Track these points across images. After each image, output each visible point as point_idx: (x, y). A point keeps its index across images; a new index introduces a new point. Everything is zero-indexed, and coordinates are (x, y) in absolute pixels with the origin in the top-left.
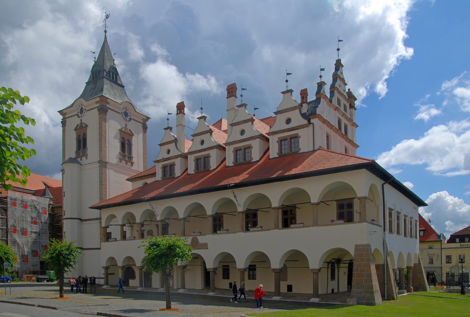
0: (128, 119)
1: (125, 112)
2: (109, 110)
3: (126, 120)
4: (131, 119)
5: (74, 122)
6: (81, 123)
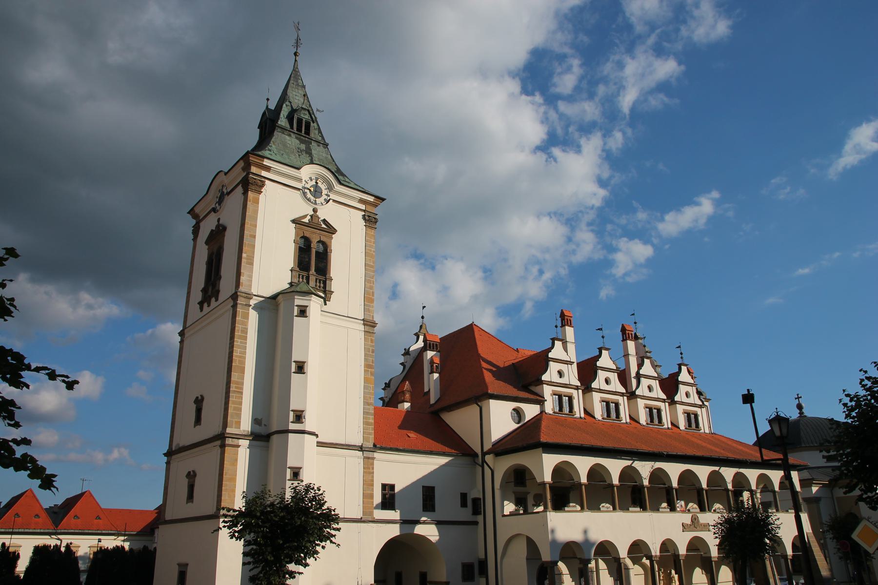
6: (218, 226)
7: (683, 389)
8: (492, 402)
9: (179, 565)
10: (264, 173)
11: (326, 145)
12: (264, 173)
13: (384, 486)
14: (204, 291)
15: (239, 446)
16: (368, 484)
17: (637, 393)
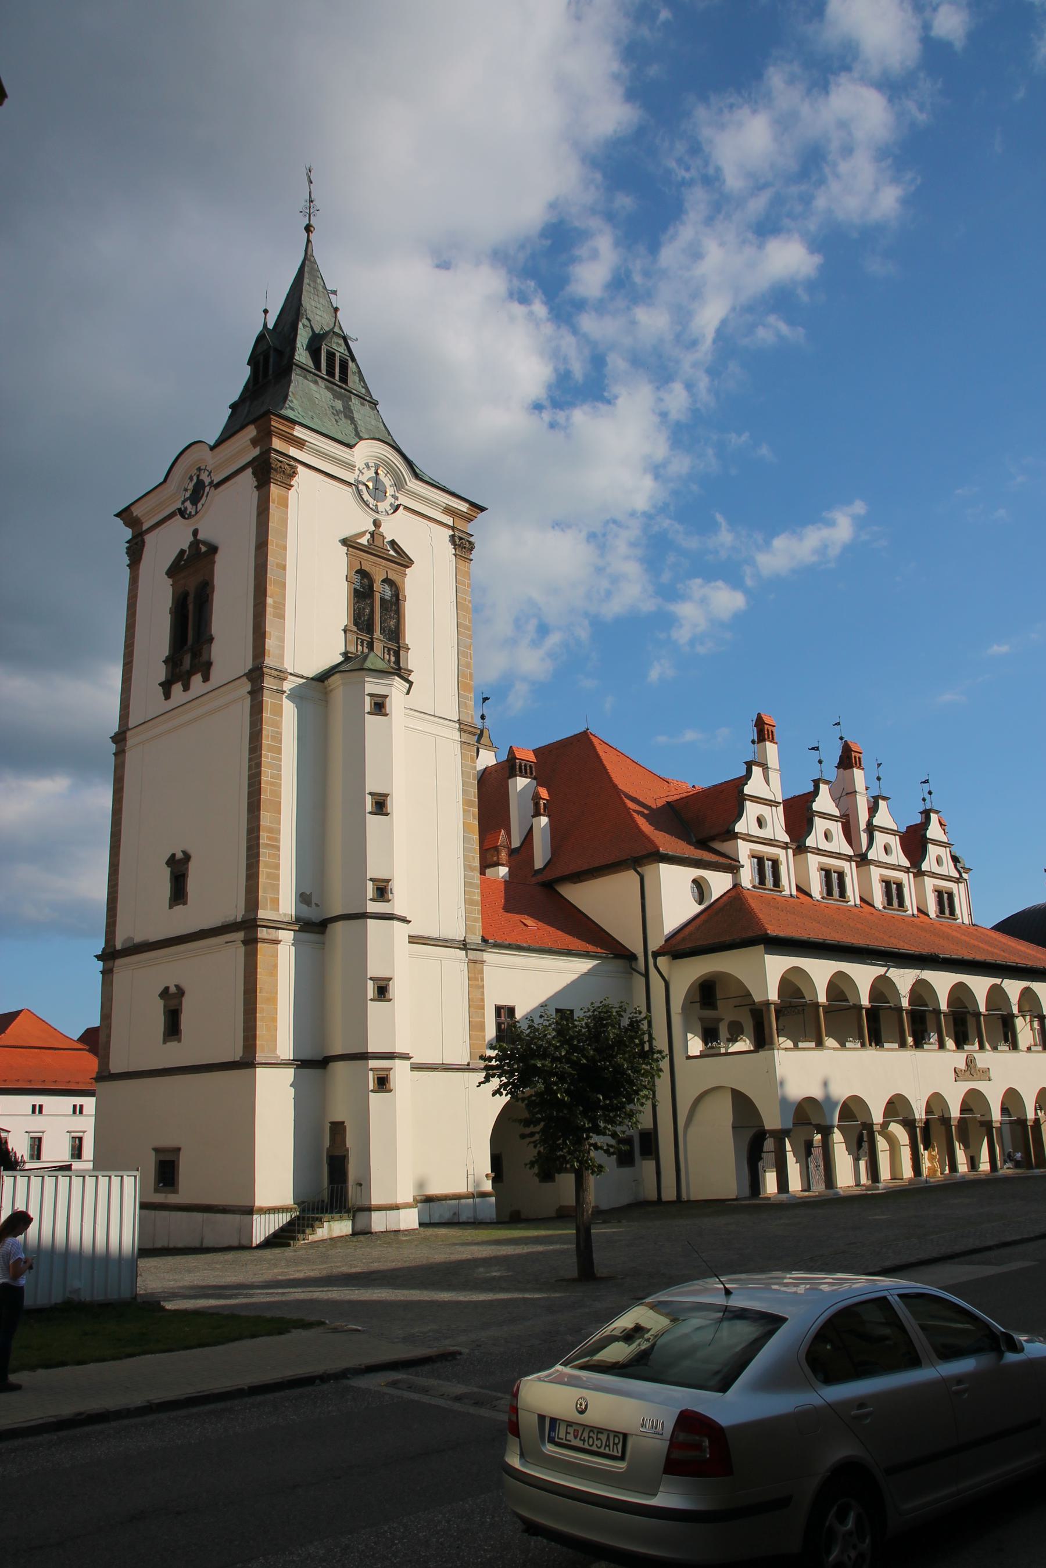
2: (300, 469)
6: (196, 543)
7: (933, 850)
8: (663, 867)
9: (157, 1150)
10: (293, 452)
11: (374, 404)
12: (293, 452)
13: (499, 1009)
14: (172, 661)
15: (278, 942)
16: (476, 1005)
17: (871, 855)
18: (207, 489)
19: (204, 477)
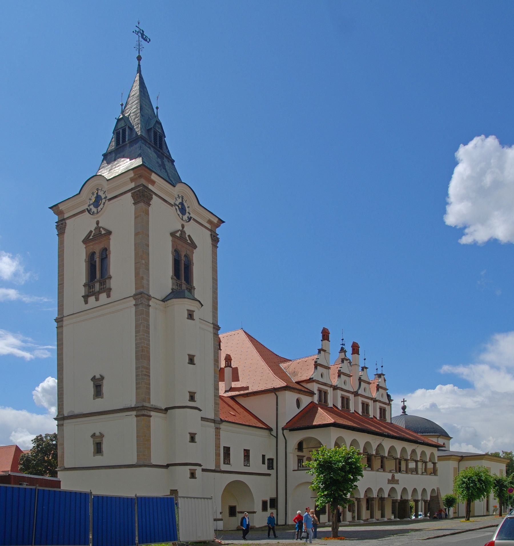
0: (185, 217)
1: (182, 204)
3: (182, 219)
4: (190, 219)
5: (81, 226)
6: (98, 228)
16: (218, 446)
18: (104, 201)
19: (101, 193)
